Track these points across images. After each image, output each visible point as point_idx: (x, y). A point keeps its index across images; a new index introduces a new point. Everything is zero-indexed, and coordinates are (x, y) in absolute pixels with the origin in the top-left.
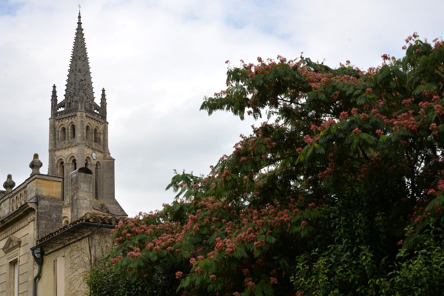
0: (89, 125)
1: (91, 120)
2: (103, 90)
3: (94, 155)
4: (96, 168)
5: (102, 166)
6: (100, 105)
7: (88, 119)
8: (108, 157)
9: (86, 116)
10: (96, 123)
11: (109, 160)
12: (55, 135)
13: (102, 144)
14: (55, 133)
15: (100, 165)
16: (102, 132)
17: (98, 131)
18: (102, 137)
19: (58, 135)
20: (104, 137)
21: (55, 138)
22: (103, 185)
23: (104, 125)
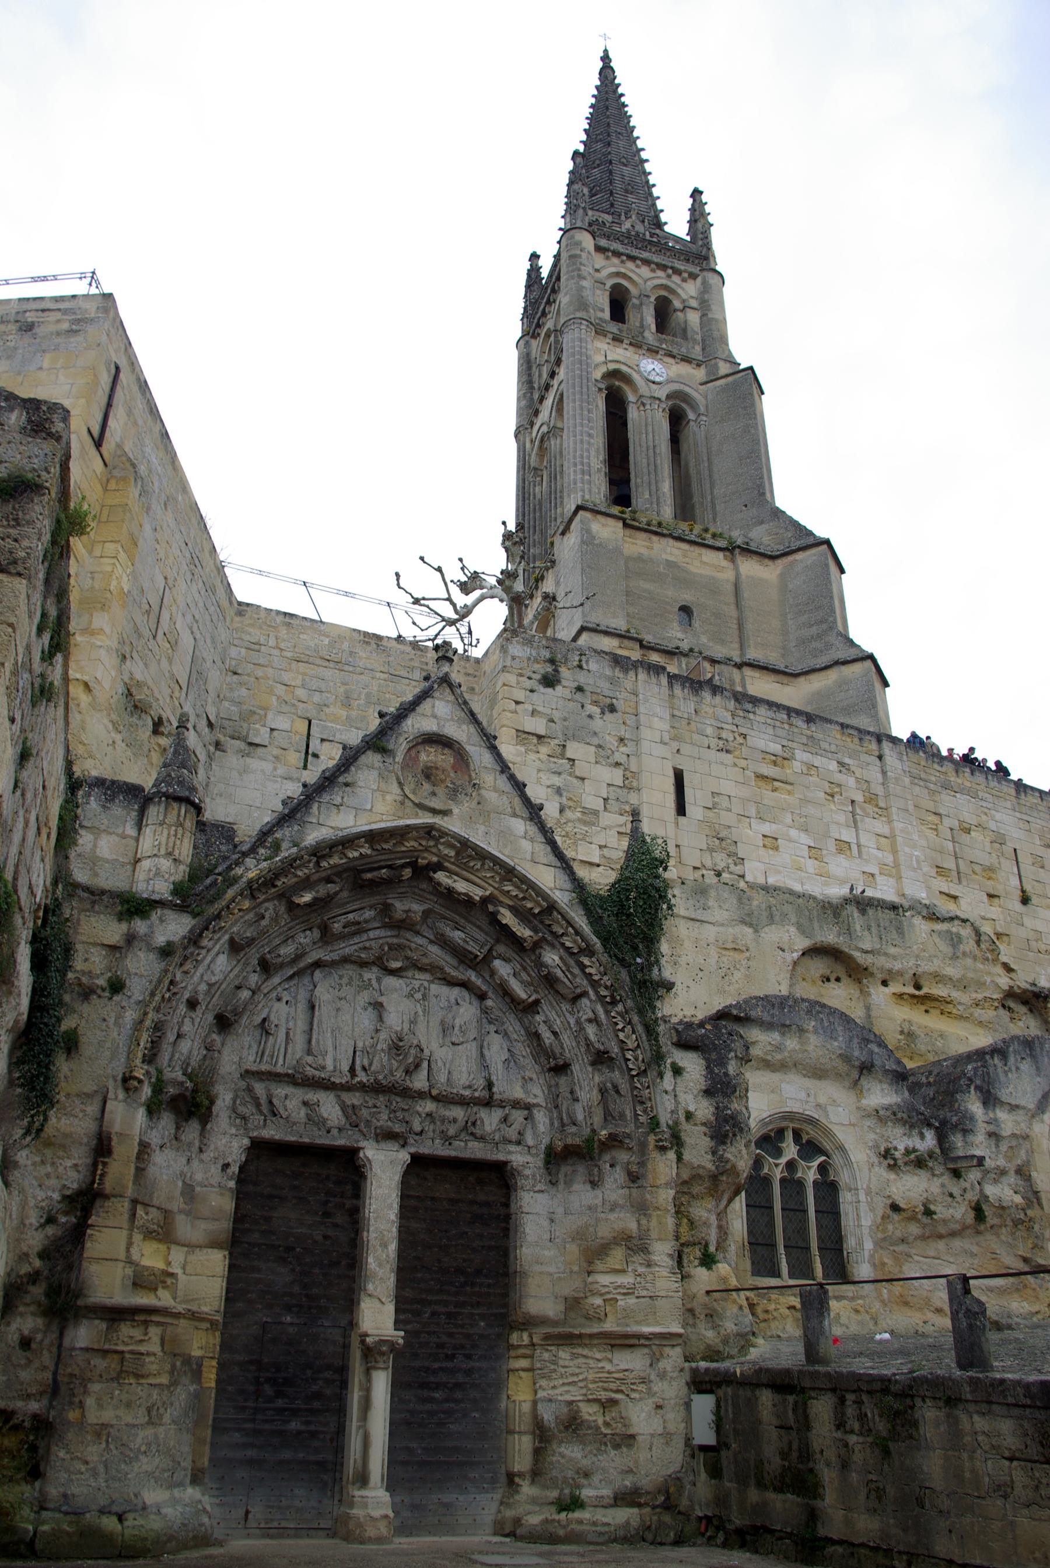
0: (625, 283)
1: (630, 265)
2: (696, 193)
3: (652, 367)
4: (677, 419)
5: (702, 409)
6: (688, 238)
7: (615, 261)
8: (724, 369)
9: (599, 249)
10: (660, 273)
11: (730, 379)
12: (530, 382)
13: (699, 338)
14: (530, 375)
15: (694, 406)
16: (694, 303)
17: (677, 304)
18: (693, 318)
19: (540, 376)
20: (703, 315)
21: (533, 388)
22: (710, 470)
23: (699, 280)
